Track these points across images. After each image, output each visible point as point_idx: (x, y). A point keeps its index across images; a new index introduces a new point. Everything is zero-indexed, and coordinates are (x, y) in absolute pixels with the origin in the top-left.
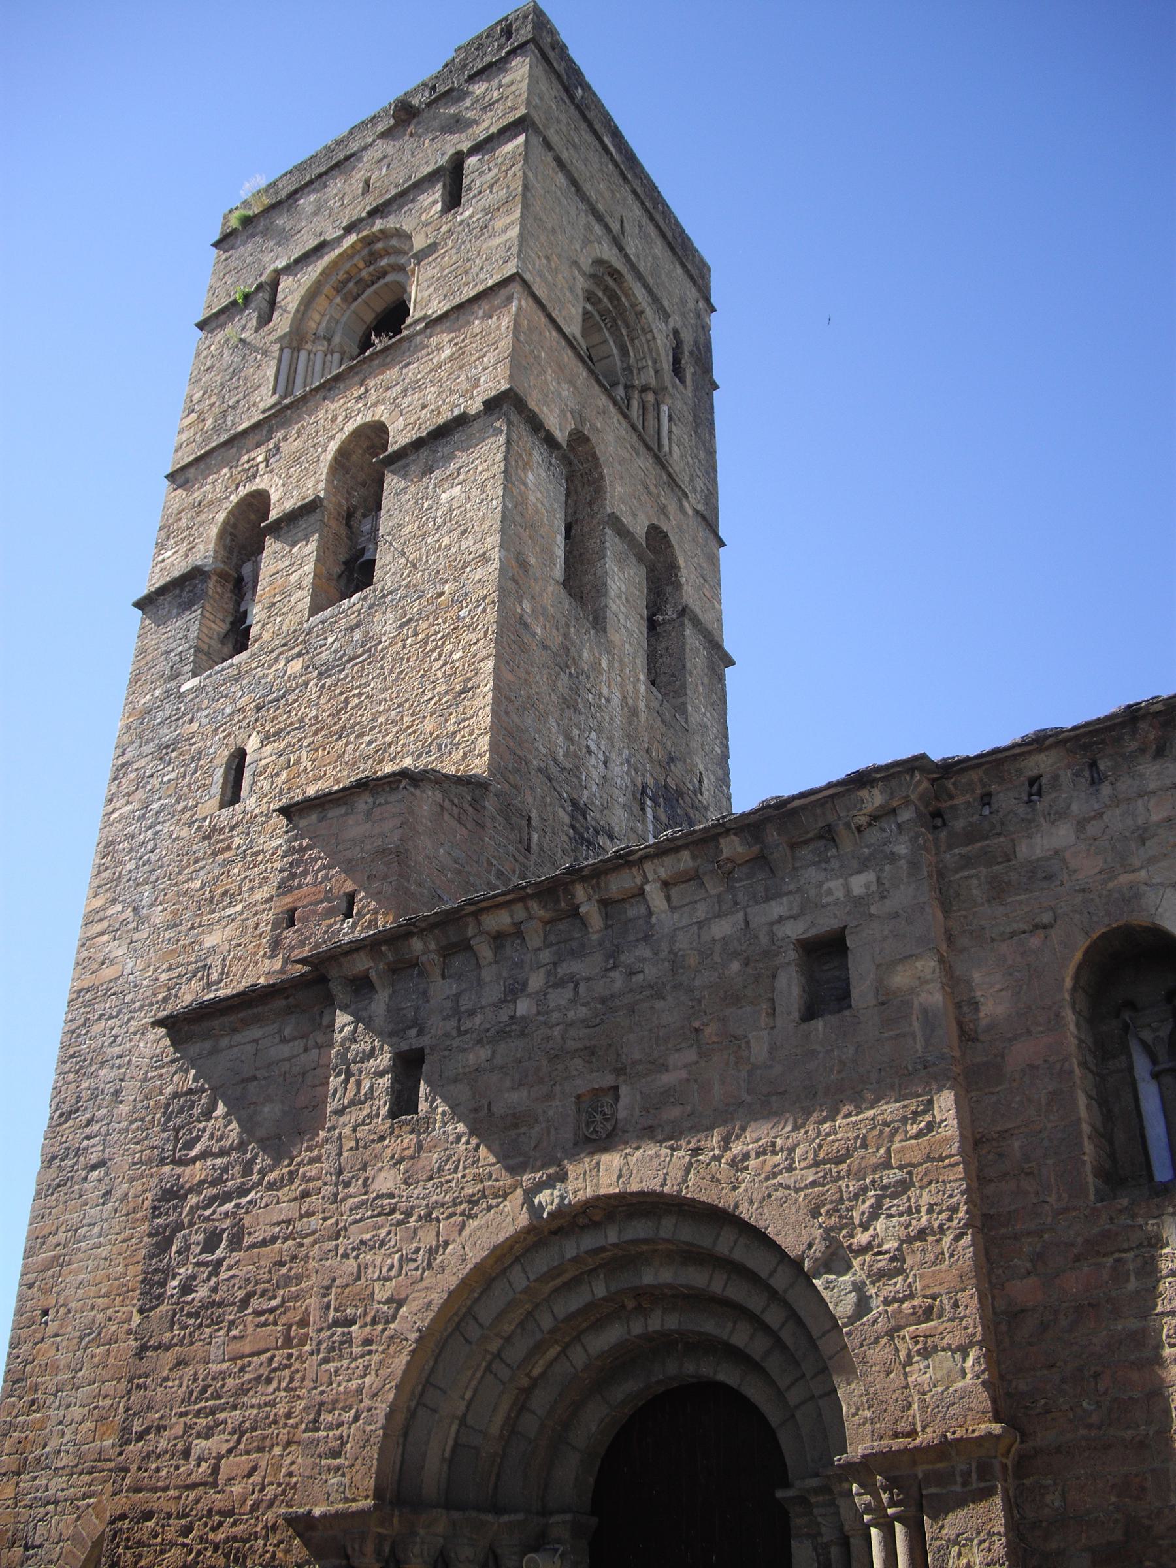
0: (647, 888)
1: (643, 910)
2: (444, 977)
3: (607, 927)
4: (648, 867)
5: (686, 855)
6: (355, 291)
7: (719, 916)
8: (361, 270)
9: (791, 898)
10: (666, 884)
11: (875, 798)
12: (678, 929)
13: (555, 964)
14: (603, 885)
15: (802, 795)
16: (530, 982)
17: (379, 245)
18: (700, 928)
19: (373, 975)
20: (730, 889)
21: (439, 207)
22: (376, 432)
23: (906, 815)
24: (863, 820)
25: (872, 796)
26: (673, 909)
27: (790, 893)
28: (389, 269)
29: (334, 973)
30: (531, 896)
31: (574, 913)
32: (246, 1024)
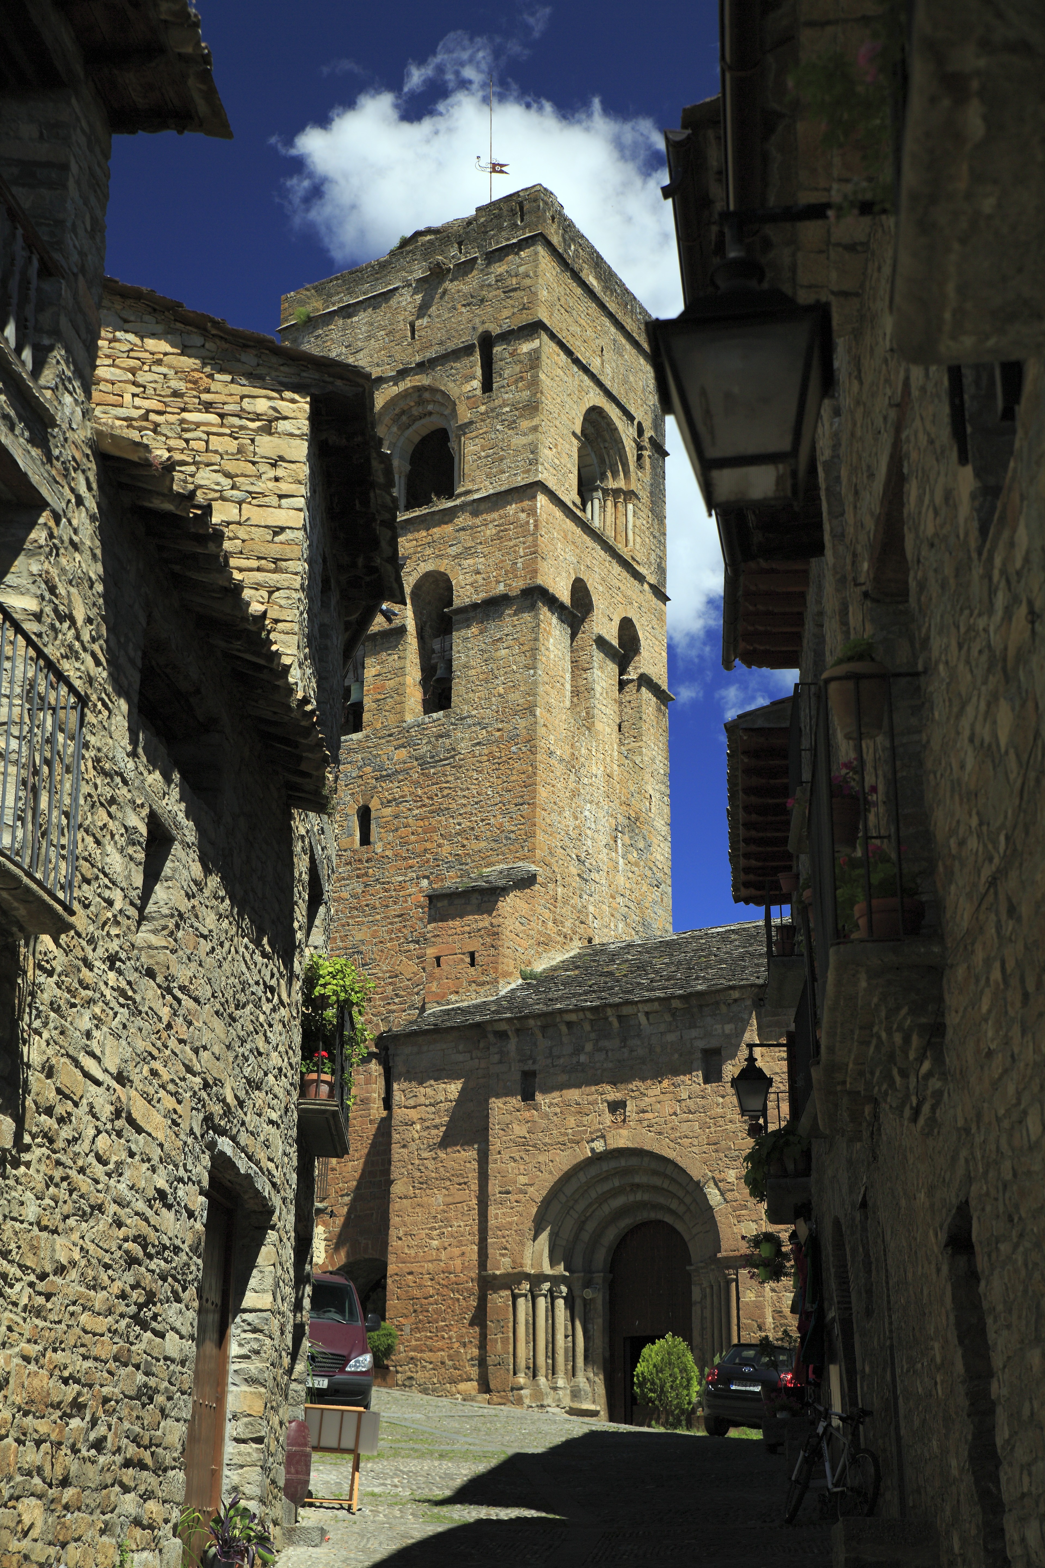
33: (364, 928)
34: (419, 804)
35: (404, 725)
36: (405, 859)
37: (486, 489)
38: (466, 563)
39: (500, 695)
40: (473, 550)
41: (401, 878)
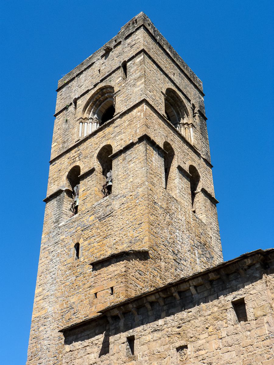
0: (191, 288)
1: (190, 294)
2: (138, 314)
3: (181, 299)
4: (190, 282)
5: (200, 278)
6: (99, 104)
7: (210, 295)
8: (100, 98)
9: (229, 290)
10: (195, 287)
11: (249, 261)
12: (200, 299)
13: (168, 310)
14: (179, 287)
15: (229, 262)
16: (162, 316)
17: (105, 90)
18: (205, 299)
19: (119, 315)
20: (212, 287)
21: (120, 78)
22: (107, 149)
23: (258, 266)
24: (246, 267)
25: (248, 261)
26: (198, 293)
27: (228, 288)
28: (108, 97)
29: (108, 315)
30: (160, 291)
31: (172, 295)
32: (85, 330)
33: (75, 296)
34: (98, 236)
35: (94, 206)
37: (125, 109)
38: (117, 138)
40: (120, 132)
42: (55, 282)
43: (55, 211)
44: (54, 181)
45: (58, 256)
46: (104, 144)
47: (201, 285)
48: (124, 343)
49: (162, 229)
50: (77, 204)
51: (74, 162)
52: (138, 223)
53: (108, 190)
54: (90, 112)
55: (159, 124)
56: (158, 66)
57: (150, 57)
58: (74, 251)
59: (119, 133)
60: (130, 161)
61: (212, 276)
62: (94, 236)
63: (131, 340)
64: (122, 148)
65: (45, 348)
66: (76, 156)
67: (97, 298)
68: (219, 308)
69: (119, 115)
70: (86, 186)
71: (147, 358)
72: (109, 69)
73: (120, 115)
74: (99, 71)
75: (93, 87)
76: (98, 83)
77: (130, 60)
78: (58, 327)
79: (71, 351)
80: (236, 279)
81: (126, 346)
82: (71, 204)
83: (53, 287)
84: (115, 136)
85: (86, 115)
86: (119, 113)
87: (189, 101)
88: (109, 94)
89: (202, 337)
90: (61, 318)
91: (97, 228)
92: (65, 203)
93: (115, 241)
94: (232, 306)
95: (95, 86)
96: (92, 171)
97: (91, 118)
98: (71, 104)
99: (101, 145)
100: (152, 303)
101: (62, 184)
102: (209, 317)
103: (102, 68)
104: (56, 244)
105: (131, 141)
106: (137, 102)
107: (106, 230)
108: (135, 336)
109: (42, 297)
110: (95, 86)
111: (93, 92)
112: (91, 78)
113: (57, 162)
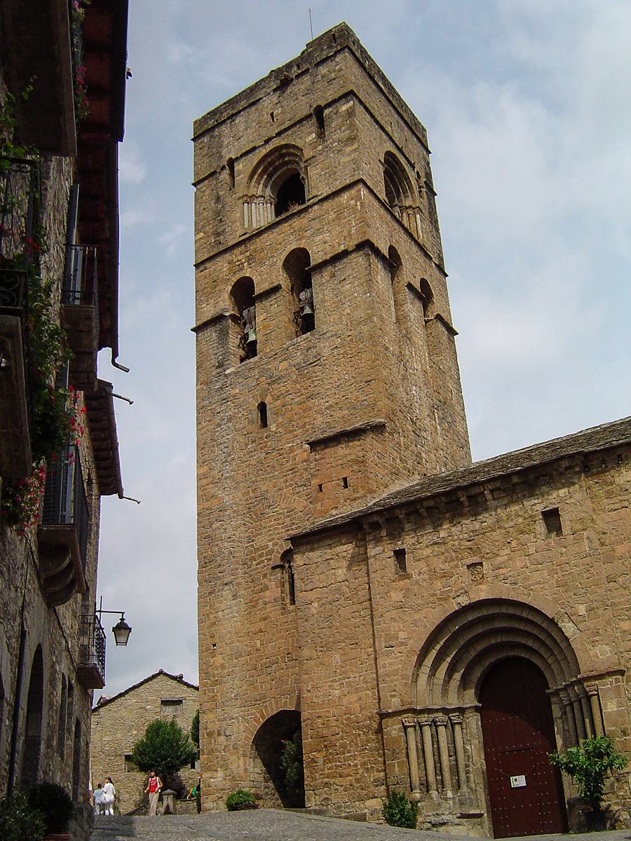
0: (486, 492)
10: (492, 491)
21: (314, 135)
30: (442, 495)
36: (291, 431)
37: (326, 191)
38: (317, 239)
39: (348, 314)
41: (290, 445)
42: (229, 459)
43: (215, 348)
44: (206, 298)
45: (230, 420)
46: (294, 246)
47: (499, 489)
48: (389, 558)
49: (397, 388)
50: (252, 338)
51: (242, 269)
52: (365, 379)
53: (306, 323)
54: (259, 184)
55: (381, 217)
56: (372, 116)
57: (361, 103)
58: (256, 415)
59: (319, 231)
60: (343, 280)
61: (515, 480)
62: (290, 394)
63: (400, 555)
64: (328, 257)
65: (226, 551)
66: (243, 260)
67: (322, 491)
68: (525, 519)
69: (316, 200)
70: (267, 312)
71: (427, 577)
72: (289, 116)
73: (320, 201)
74: (272, 115)
75: (263, 143)
76: (273, 137)
77: (329, 105)
78: (244, 524)
79: (305, 564)
80: (548, 484)
81: (392, 562)
82: (239, 337)
83: (228, 467)
84: (312, 235)
85: (253, 191)
86: (316, 196)
87: (413, 166)
88: (291, 158)
89: (502, 553)
90: (247, 512)
91: (296, 382)
92: (230, 336)
93: (327, 404)
94: (542, 517)
95: (267, 142)
96: (276, 289)
97: (262, 196)
98: (223, 168)
99: (289, 246)
100: (428, 509)
101: (222, 305)
102: (511, 529)
103: (276, 111)
104: (224, 401)
105: (342, 248)
106: (348, 182)
107: (310, 386)
108: (406, 550)
109: (210, 480)
110: (267, 142)
111: (264, 151)
112: (257, 127)
113: (208, 265)
